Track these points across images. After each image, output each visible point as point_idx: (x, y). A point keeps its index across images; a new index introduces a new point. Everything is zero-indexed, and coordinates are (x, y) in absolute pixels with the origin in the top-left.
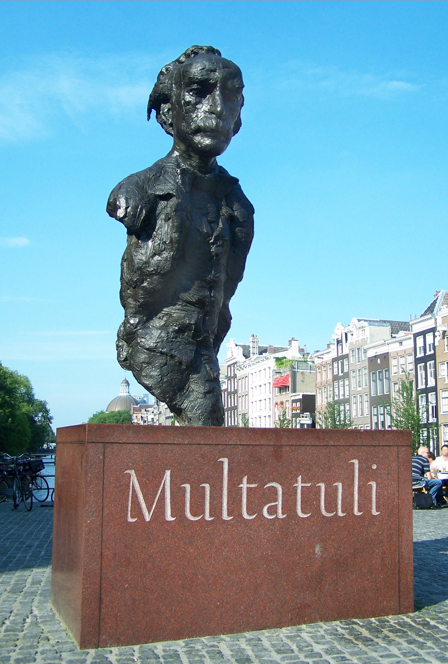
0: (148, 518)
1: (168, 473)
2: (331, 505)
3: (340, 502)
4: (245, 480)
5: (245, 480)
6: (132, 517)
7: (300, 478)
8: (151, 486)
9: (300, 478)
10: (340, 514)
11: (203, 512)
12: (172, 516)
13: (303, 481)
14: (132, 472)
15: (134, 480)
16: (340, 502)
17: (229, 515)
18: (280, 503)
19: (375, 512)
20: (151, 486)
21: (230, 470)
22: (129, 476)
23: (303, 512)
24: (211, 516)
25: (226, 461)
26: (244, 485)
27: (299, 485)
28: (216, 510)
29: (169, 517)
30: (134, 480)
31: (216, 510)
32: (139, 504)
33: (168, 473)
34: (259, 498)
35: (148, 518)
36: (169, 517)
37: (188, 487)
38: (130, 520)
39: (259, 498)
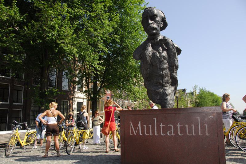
0: (135, 134)
1: (140, 122)
2: (190, 131)
3: (193, 131)
4: (161, 124)
5: (161, 124)
6: (131, 134)
7: (179, 123)
8: (136, 126)
9: (179, 123)
10: (194, 134)
11: (150, 133)
12: (141, 134)
13: (180, 124)
14: (131, 122)
15: (131, 124)
16: (193, 131)
17: (157, 134)
18: (173, 131)
19: (207, 135)
20: (136, 126)
21: (157, 121)
22: (130, 123)
23: (181, 133)
24: (152, 134)
25: (155, 119)
26: (161, 126)
27: (179, 125)
28: (153, 132)
29: (141, 134)
30: (131, 124)
31: (153, 132)
32: (133, 131)
33: (140, 122)
34: (166, 129)
35: (135, 134)
36: (141, 134)
37: (145, 126)
38: (131, 134)
39: (166, 129)
